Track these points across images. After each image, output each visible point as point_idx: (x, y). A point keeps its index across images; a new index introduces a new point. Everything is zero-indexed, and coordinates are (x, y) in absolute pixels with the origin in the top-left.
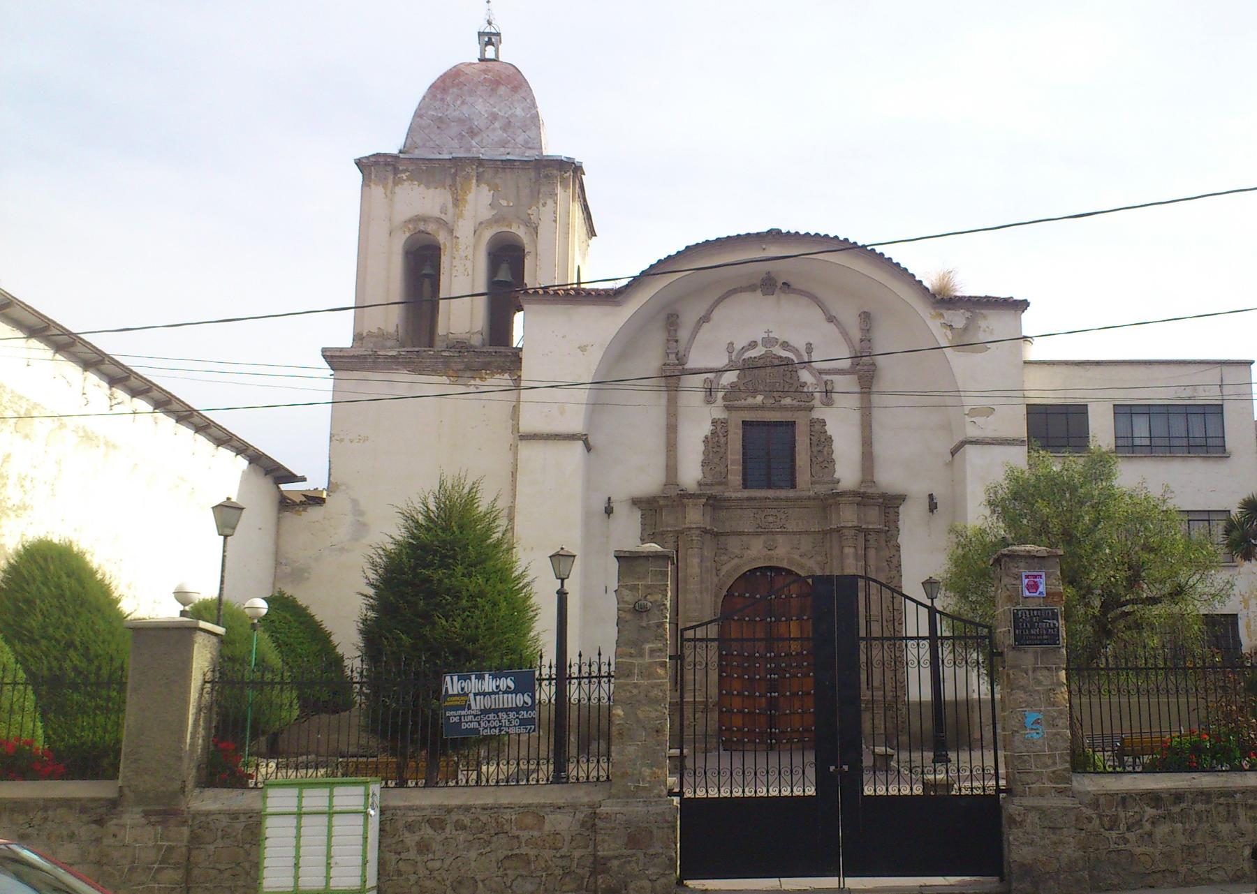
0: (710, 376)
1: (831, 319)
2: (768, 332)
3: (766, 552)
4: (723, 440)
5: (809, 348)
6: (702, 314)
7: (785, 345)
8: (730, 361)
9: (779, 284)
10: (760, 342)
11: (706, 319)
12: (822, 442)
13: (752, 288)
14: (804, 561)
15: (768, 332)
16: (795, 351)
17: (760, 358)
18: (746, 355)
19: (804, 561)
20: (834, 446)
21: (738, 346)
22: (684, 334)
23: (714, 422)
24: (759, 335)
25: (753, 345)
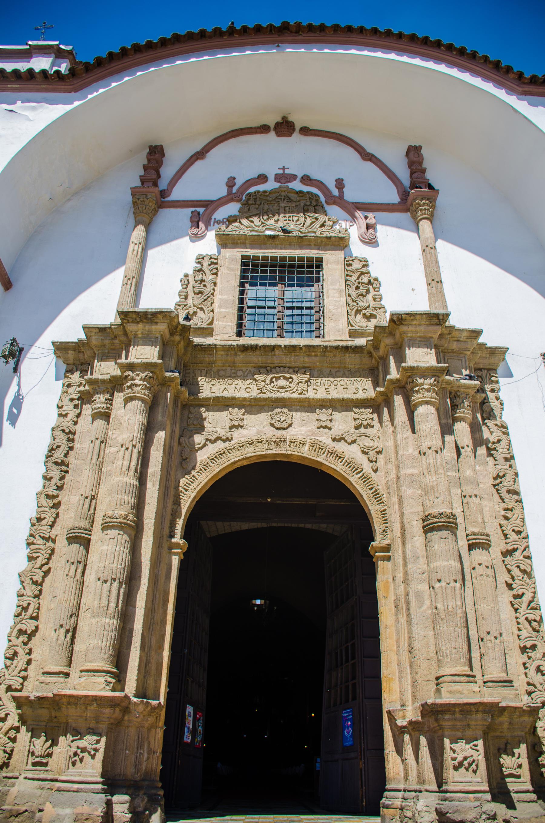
0: (201, 210)
1: (367, 157)
2: (284, 168)
3: (271, 432)
4: (209, 277)
5: (340, 184)
6: (199, 148)
7: (306, 180)
8: (230, 193)
9: (297, 129)
10: (271, 178)
11: (200, 155)
12: (362, 282)
13: (264, 129)
14: (341, 447)
15: (284, 168)
16: (320, 185)
17: (271, 192)
18: (252, 190)
19: (341, 447)
20: (383, 291)
21: (239, 182)
22: (168, 171)
23: (200, 259)
24: (272, 172)
25: (263, 178)
